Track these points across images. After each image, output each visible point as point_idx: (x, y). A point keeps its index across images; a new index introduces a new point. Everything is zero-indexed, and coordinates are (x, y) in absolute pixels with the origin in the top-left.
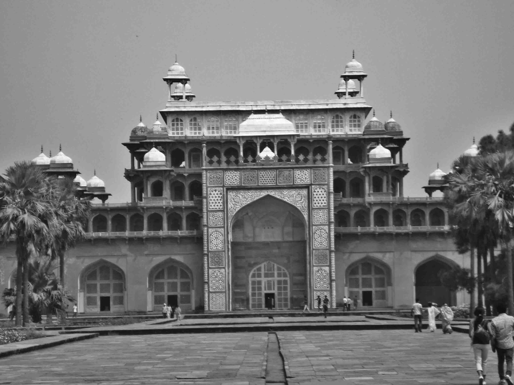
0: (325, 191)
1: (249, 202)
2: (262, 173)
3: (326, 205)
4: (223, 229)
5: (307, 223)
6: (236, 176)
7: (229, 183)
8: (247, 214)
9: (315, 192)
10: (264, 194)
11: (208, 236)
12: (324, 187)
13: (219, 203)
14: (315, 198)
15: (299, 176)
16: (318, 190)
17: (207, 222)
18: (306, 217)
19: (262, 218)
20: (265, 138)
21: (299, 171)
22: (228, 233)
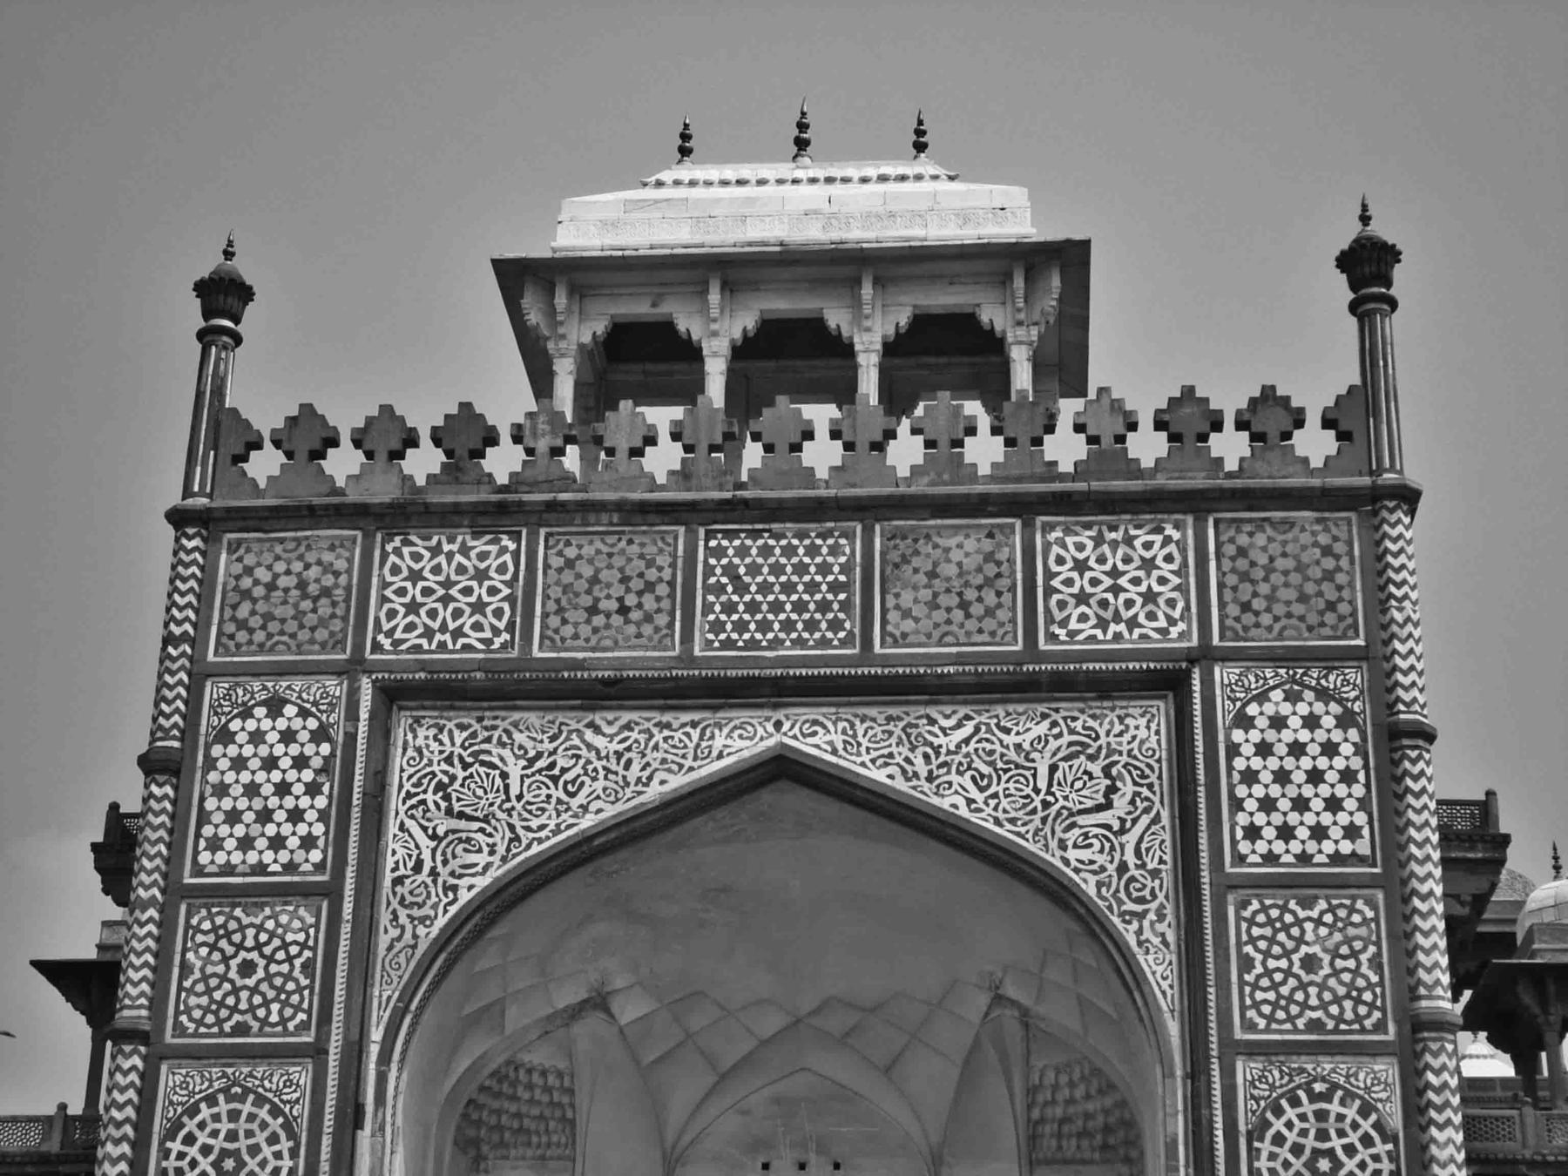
0: (1345, 721)
1: (587, 822)
2: (737, 549)
3: (1363, 847)
4: (302, 1075)
5: (1173, 1028)
6: (481, 576)
7: (413, 638)
8: (599, 1002)
9: (1245, 722)
10: (740, 740)
11: (140, 1145)
12: (1333, 680)
13: (296, 816)
14: (1250, 777)
15: (1081, 583)
16: (1278, 702)
17: (157, 1004)
18: (1159, 969)
19: (746, 1062)
20: (783, 304)
21: (1086, 537)
22: (351, 1116)
